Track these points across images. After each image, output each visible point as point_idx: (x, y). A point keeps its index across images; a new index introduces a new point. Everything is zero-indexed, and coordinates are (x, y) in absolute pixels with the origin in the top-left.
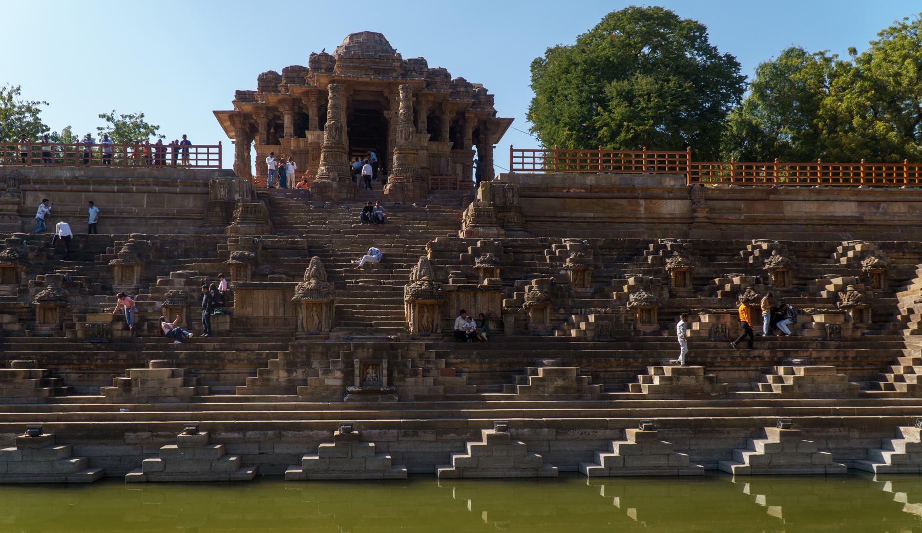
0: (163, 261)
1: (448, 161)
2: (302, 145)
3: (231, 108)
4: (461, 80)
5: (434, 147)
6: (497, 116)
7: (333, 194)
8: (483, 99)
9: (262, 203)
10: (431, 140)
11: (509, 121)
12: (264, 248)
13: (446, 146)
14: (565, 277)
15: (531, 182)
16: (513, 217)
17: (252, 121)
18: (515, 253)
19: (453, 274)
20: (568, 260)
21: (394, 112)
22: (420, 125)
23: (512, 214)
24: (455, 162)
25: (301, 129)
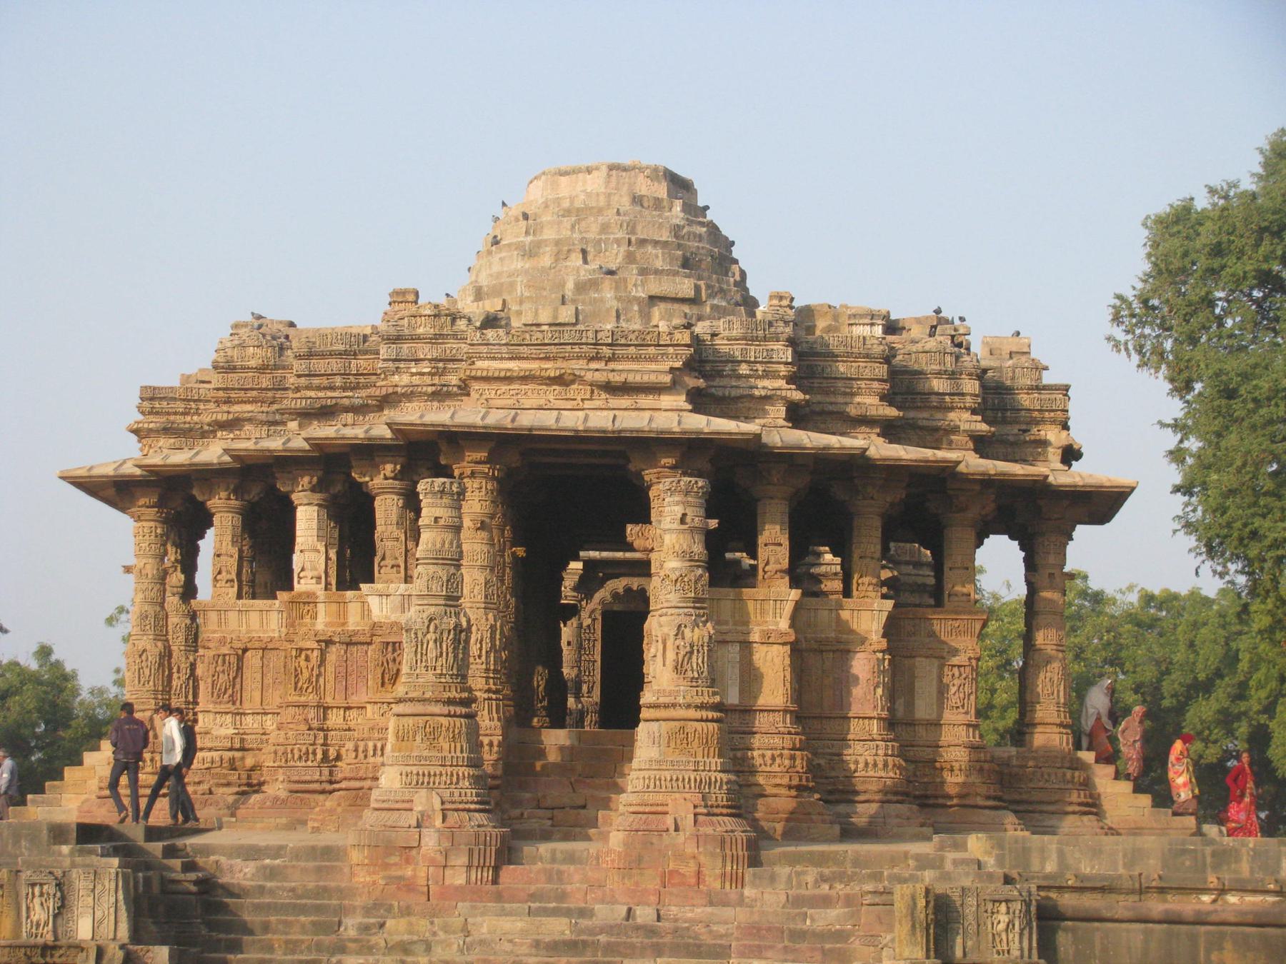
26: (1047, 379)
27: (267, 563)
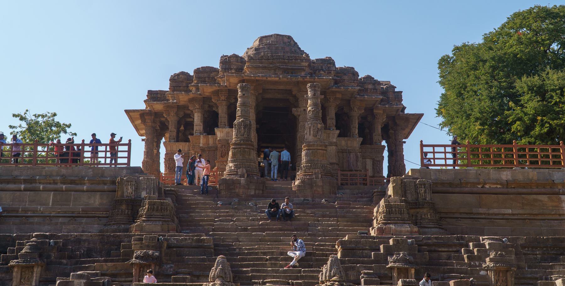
0: (64, 261)
1: (357, 157)
2: (211, 141)
3: (143, 107)
4: (369, 78)
5: (343, 143)
6: (406, 112)
7: (241, 191)
8: (391, 96)
9: (169, 201)
10: (339, 136)
11: (418, 117)
12: (169, 247)
13: (356, 142)
14: (486, 277)
15: (444, 177)
16: (426, 214)
17: (163, 119)
18: (430, 251)
19: (365, 274)
20: (488, 259)
21: (302, 109)
22: (329, 122)
23: (425, 210)
24: (364, 158)
25: (210, 126)
26: (396, 90)
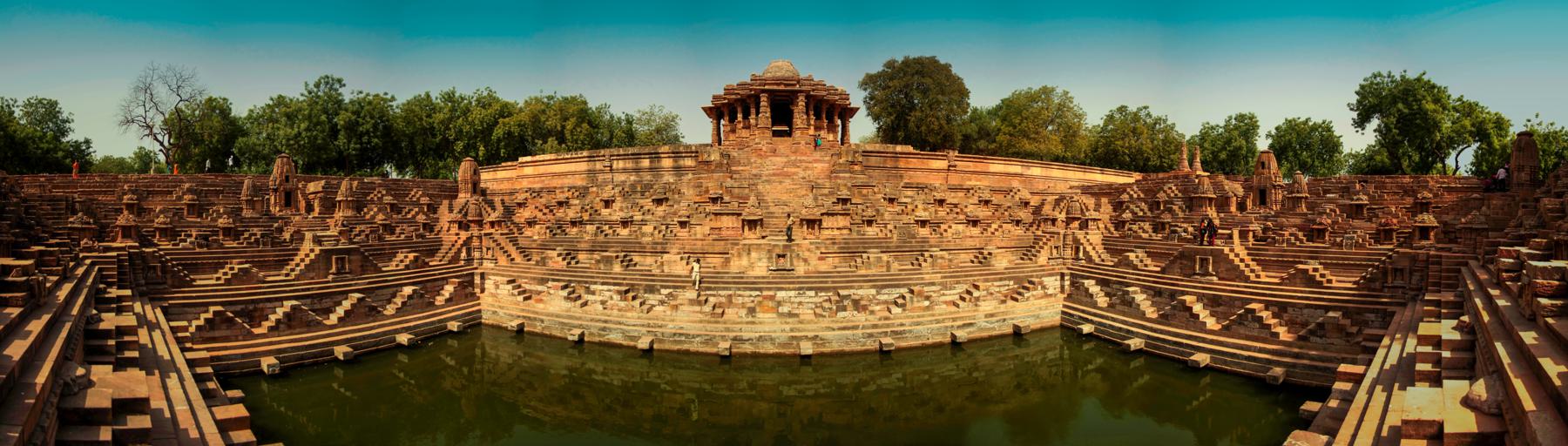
27: (733, 119)
